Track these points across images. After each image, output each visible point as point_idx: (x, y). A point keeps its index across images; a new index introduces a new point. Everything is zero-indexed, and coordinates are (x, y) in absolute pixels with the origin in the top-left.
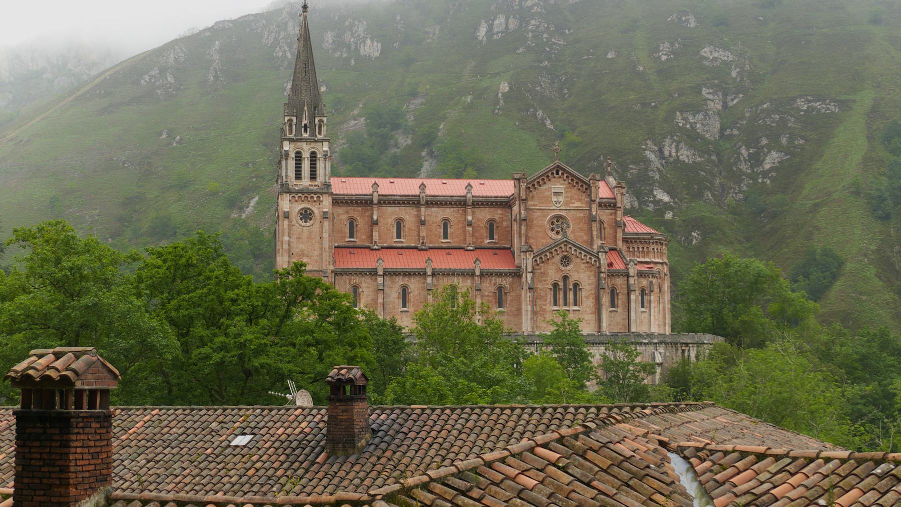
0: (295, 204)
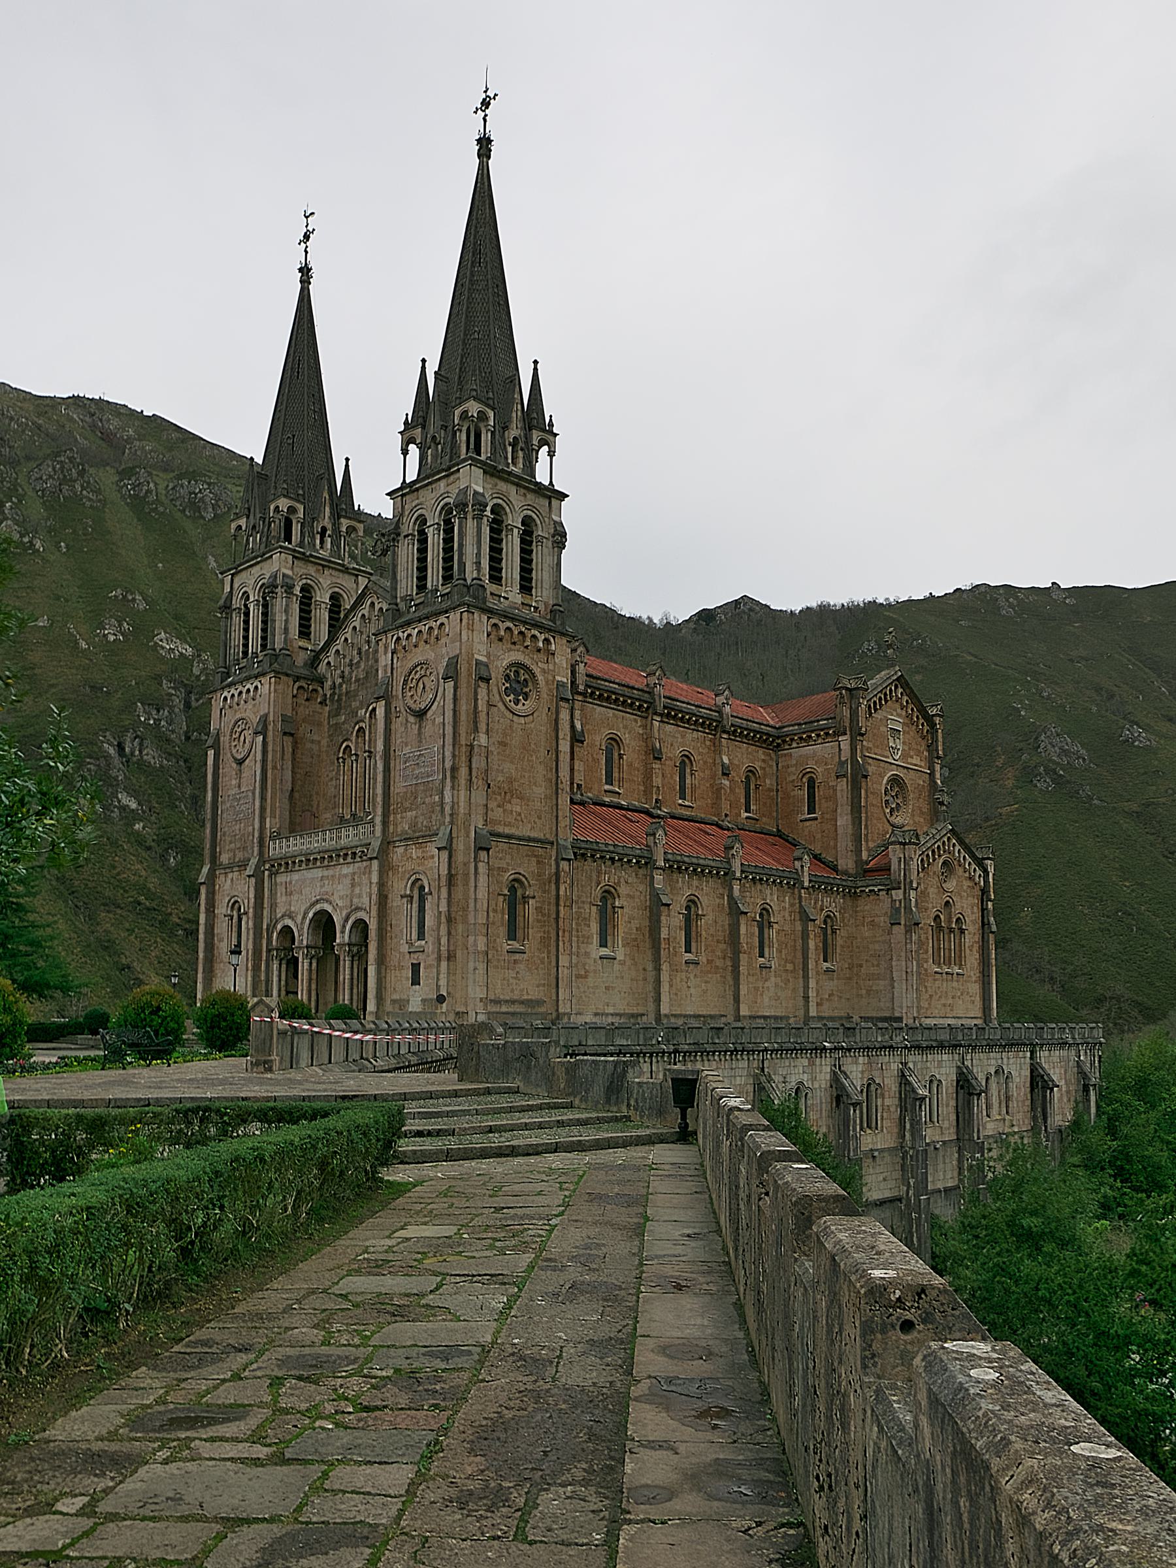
0: (498, 648)
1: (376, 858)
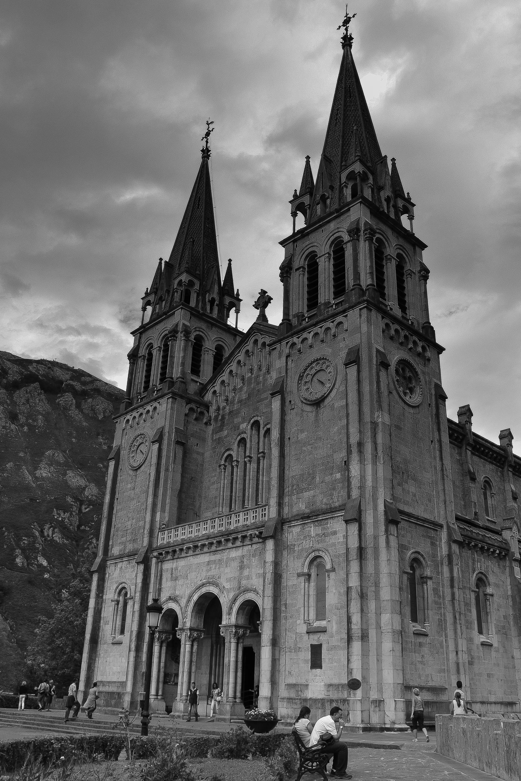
1: (272, 537)
